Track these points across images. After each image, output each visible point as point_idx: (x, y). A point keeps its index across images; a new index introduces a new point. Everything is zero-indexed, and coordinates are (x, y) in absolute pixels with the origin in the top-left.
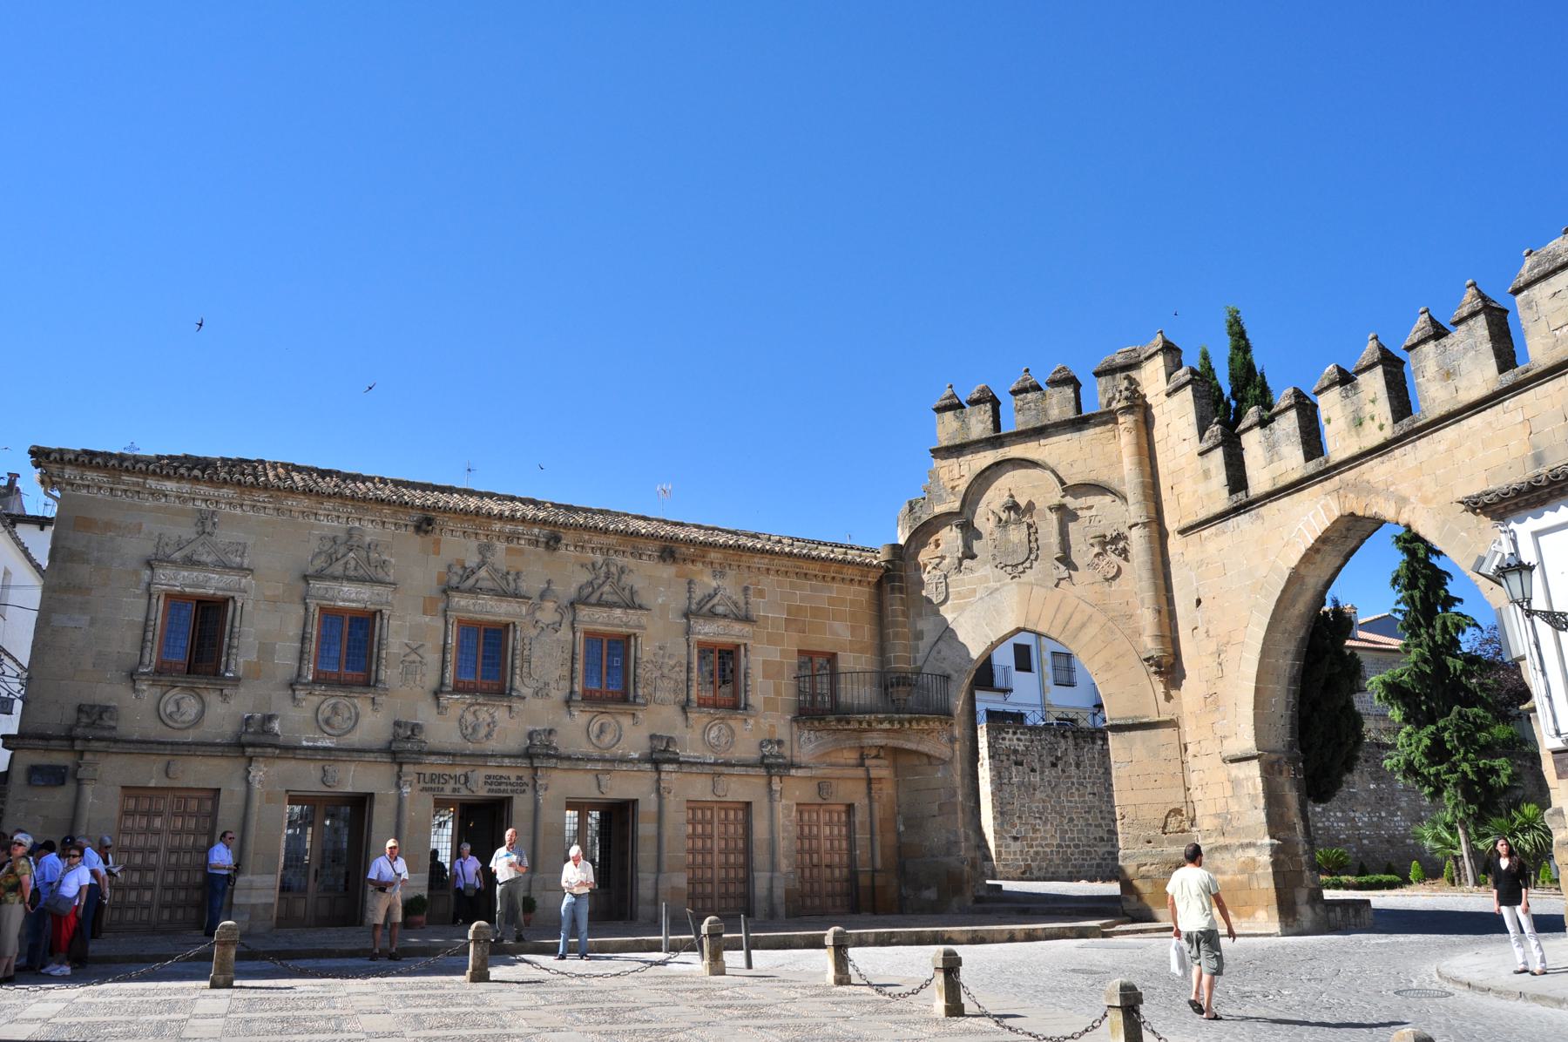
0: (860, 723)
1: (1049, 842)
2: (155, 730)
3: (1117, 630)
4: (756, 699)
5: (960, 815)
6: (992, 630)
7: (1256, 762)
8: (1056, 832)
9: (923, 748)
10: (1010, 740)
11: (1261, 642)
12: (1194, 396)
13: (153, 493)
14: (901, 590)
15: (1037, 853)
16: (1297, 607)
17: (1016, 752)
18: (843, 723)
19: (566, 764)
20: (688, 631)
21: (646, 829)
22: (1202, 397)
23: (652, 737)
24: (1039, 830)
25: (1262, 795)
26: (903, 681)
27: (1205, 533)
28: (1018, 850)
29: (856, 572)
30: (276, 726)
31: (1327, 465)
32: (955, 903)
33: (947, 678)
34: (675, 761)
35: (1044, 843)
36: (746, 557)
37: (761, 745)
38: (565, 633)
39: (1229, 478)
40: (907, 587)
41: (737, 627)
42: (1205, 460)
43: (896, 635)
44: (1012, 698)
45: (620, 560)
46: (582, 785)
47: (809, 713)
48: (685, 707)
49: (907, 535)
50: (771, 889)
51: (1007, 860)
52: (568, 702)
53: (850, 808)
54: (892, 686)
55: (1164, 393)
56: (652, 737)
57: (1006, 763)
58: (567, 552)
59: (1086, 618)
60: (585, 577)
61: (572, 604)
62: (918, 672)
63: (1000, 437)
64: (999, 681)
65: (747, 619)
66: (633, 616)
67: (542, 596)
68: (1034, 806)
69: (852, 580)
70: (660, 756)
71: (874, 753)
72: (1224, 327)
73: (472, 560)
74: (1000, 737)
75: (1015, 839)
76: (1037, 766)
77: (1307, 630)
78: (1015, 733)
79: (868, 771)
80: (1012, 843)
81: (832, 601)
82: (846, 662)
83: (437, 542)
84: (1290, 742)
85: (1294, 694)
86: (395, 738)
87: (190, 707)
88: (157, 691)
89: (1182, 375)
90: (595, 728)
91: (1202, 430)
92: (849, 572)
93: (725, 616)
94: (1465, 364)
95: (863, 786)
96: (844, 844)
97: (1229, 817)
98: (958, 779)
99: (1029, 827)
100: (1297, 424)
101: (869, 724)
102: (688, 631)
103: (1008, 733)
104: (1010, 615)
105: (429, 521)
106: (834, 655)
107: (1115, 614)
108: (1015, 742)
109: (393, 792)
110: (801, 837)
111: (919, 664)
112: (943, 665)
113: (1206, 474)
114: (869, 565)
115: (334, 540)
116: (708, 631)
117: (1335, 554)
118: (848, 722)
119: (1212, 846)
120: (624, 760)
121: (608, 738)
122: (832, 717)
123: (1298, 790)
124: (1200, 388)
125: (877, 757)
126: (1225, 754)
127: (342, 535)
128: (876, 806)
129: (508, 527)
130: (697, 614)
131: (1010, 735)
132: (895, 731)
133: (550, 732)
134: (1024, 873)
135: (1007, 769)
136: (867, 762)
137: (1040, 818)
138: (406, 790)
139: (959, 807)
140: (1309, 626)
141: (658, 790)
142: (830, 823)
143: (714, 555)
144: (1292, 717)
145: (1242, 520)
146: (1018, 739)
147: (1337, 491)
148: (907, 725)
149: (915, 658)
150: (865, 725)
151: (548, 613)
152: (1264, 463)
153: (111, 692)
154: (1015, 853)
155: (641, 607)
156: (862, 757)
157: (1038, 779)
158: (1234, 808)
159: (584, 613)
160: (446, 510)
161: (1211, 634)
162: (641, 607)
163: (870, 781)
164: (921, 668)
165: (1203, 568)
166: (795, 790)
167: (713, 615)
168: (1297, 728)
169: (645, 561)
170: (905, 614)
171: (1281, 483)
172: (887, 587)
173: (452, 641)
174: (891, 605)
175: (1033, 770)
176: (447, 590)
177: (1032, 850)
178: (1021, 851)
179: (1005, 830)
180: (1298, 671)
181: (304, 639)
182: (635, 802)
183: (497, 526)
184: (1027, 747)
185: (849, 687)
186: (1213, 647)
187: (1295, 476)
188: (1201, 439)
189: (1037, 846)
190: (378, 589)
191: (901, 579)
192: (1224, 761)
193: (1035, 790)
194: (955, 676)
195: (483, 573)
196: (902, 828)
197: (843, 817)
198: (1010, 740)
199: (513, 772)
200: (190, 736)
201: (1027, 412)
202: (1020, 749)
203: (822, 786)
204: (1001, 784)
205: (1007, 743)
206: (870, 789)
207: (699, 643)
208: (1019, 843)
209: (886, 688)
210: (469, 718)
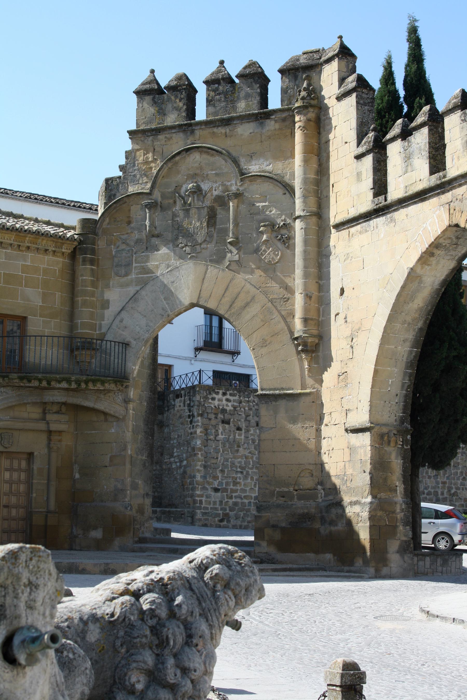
0: (40, 381)
1: (248, 494)
3: (275, 311)
5: (128, 466)
6: (167, 303)
7: (367, 435)
8: (255, 485)
9: (100, 406)
10: (219, 400)
11: (382, 330)
12: (357, 103)
14: (92, 262)
15: (235, 504)
16: (416, 301)
17: (224, 411)
18: (25, 381)
22: (365, 104)
24: (239, 483)
25: (369, 461)
27: (353, 230)
28: (218, 500)
29: (50, 243)
31: (443, 180)
32: (117, 542)
33: (126, 345)
35: (243, 495)
39: (375, 182)
40: (98, 259)
42: (360, 163)
43: (85, 303)
44: (239, 360)
49: (103, 211)
51: (207, 508)
53: (30, 455)
54: (78, 349)
55: (335, 96)
57: (213, 422)
59: (249, 299)
62: (102, 338)
63: (190, 125)
64: (228, 345)
68: (236, 461)
69: (46, 250)
71: (55, 408)
72: (405, 35)
74: (210, 397)
75: (216, 490)
76: (243, 425)
77: (425, 322)
78: (224, 394)
79: (48, 423)
80: (213, 493)
81: (25, 269)
84: (401, 417)
85: (410, 377)
89: (351, 82)
91: (360, 138)
92: (43, 243)
95: (44, 438)
96: (22, 488)
97: (346, 478)
98: (129, 435)
99: (230, 480)
100: (427, 140)
101: (49, 383)
103: (217, 393)
104: (185, 291)
106: (24, 319)
107: (275, 296)
108: (224, 402)
111: (103, 330)
112: (124, 333)
113: (359, 175)
114: (63, 238)
117: (449, 257)
118: (30, 381)
119: (331, 502)
122: (15, 375)
123: (404, 458)
124: (364, 96)
125: (57, 412)
126: (347, 426)
128: (54, 455)
131: (220, 396)
132: (73, 390)
134: (221, 521)
135: (215, 426)
136: (49, 417)
137: (242, 473)
139: (128, 460)
140: (427, 319)
144: (406, 396)
145: (380, 221)
146: (228, 400)
147: (449, 203)
148: (83, 386)
149: (100, 325)
150: (44, 384)
152: (400, 173)
154: (215, 503)
156: (44, 413)
157: (243, 437)
158: (349, 471)
161: (348, 319)
164: (104, 335)
165: (348, 261)
168: (410, 407)
170: (94, 284)
171: (411, 192)
172: (80, 258)
174: (82, 275)
175: (239, 429)
177: (231, 502)
178: (221, 502)
179: (209, 483)
180: (415, 357)
184: (235, 408)
185: (38, 348)
186: (348, 333)
187: (420, 187)
188: (359, 144)
189: (236, 497)
191: (93, 252)
192: (346, 430)
193: (239, 446)
194: (133, 343)
196: (77, 476)
197: (24, 464)
198: (219, 400)
201: (217, 104)
202: (228, 409)
204: (207, 440)
205: (216, 403)
206: (49, 440)
208: (219, 494)
209: (72, 351)
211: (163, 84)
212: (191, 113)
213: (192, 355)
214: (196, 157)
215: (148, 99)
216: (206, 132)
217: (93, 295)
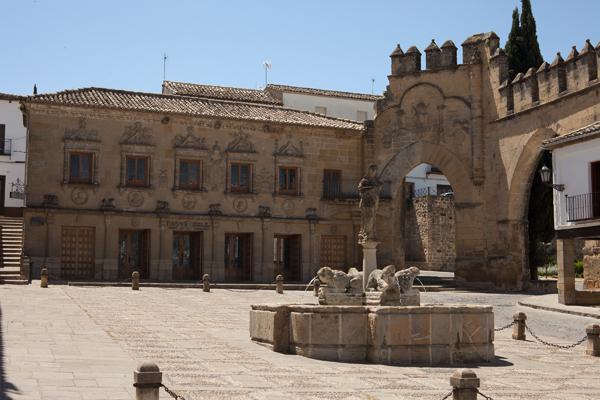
2: (70, 204)
4: (305, 191)
13: (62, 111)
14: (372, 142)
17: (442, 209)
19: (225, 218)
20: (275, 162)
21: (257, 244)
23: (260, 207)
30: (114, 203)
34: (269, 217)
36: (300, 129)
37: (307, 211)
38: (223, 164)
41: (297, 160)
45: (245, 131)
46: (230, 226)
47: (327, 196)
48: (274, 194)
50: (310, 270)
52: (225, 193)
56: (260, 207)
58: (224, 129)
60: (231, 139)
61: (226, 151)
65: (301, 156)
66: (251, 156)
67: (215, 147)
70: (264, 214)
73: (185, 134)
75: (439, 251)
82: (346, 174)
83: (171, 127)
86: (158, 208)
87: (84, 196)
88: (70, 190)
90: (236, 204)
93: (292, 155)
94: (581, 74)
98: (392, 226)
102: (275, 162)
105: (168, 119)
109: (158, 229)
110: (323, 249)
115: (130, 127)
116: (285, 162)
120: (248, 217)
121: (242, 207)
123: (525, 236)
127: (134, 126)
129: (199, 120)
130: (280, 154)
133: (218, 205)
138: (163, 228)
141: (263, 230)
142: (337, 244)
143: (288, 129)
151: (216, 155)
153: (52, 191)
155: (255, 152)
159: (231, 155)
160: (174, 113)
162: (255, 152)
163: (354, 227)
166: (322, 229)
167: (287, 155)
169: (256, 132)
172: (366, 140)
173: (178, 168)
177: (447, 257)
181: (122, 169)
182: (253, 233)
183: (194, 119)
188: (501, 84)
190: (149, 148)
191: (372, 136)
195: (189, 139)
200: (84, 206)
203: (334, 228)
207: (280, 167)
210: (186, 199)
211: (405, 52)
212: (419, 65)
213: (424, 176)
214: (421, 88)
215: (397, 60)
216: (428, 75)
217: (372, 157)
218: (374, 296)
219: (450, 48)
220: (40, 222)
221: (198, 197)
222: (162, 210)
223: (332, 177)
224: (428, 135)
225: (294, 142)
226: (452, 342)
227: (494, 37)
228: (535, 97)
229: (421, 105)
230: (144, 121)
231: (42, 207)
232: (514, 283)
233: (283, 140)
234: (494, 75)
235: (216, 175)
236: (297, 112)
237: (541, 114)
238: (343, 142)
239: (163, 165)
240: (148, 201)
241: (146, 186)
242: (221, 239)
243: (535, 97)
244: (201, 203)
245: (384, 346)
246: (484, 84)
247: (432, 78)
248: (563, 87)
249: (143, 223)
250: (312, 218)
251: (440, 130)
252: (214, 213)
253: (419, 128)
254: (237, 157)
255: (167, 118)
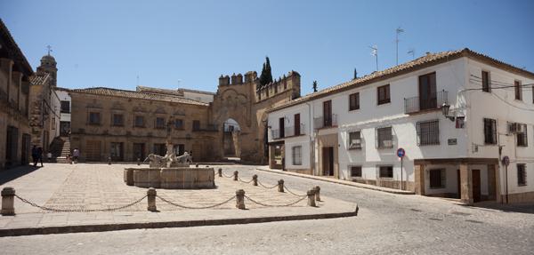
26: (212, 125)
46: (157, 141)
47: (194, 131)
82: (202, 122)
116: (177, 117)
153: (83, 127)
166: (192, 142)
176: (134, 111)
199: (145, 139)
218: (169, 164)
219: (240, 76)
220: (78, 139)
221: (143, 130)
222: (128, 135)
223: (196, 124)
224: (232, 108)
225: (182, 110)
226: (192, 181)
227: (255, 73)
228: (267, 95)
229: (230, 97)
230: (121, 101)
231: (78, 134)
232: (260, 161)
233: (177, 109)
234: (255, 86)
235: (151, 122)
236: (190, 99)
237: (269, 101)
238: (202, 111)
239: (129, 118)
240: (123, 131)
241: (122, 126)
242: (153, 146)
243: (267, 95)
244: (144, 132)
245: (165, 182)
246: (251, 89)
247: (234, 87)
248: (276, 91)
249: (121, 140)
250: (189, 138)
251: (236, 106)
252: (150, 136)
253: (228, 106)
254: (159, 115)
255: (130, 100)
